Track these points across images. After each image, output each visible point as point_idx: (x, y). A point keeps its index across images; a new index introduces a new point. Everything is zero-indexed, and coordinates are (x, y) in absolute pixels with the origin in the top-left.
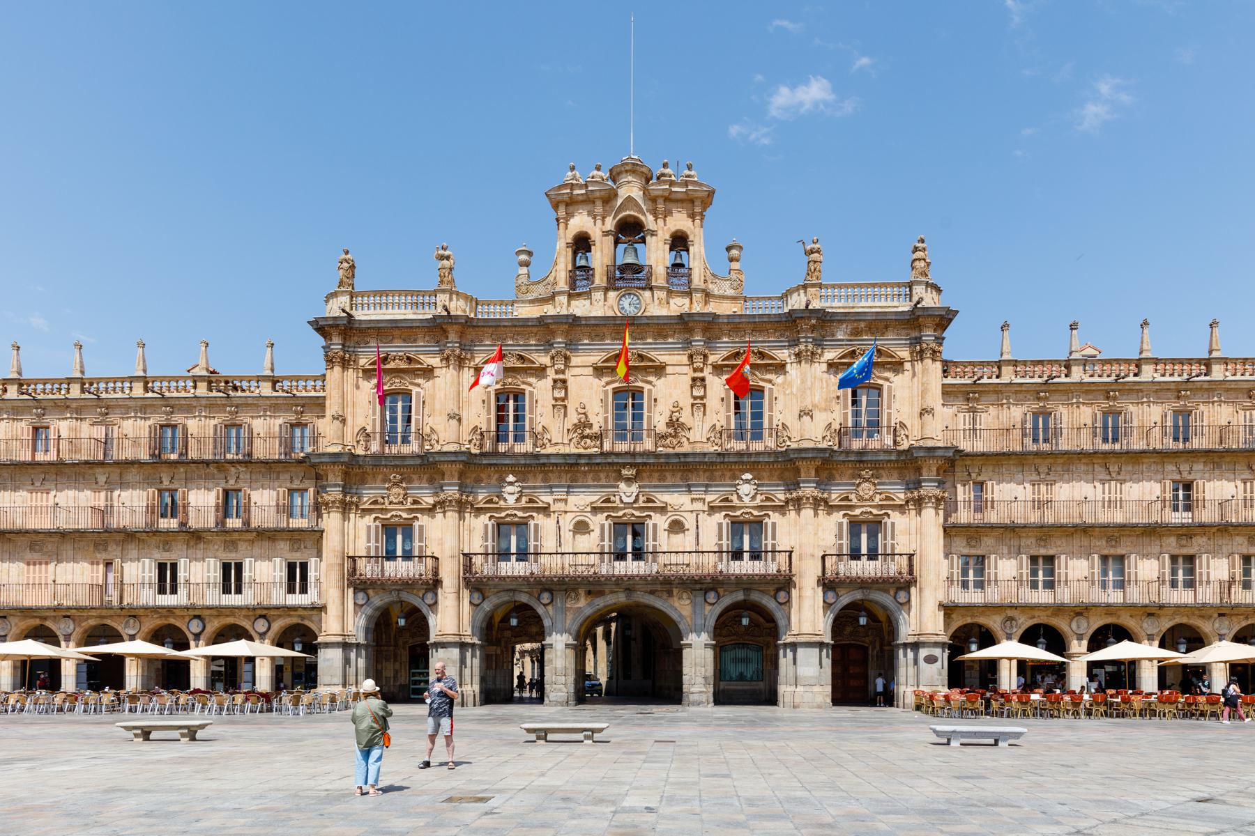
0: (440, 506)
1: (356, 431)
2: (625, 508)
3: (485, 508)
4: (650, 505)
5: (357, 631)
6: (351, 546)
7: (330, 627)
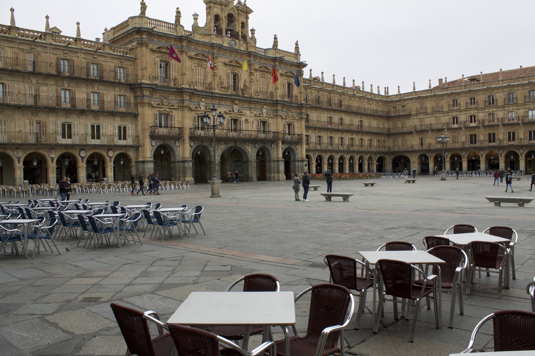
0: (182, 107)
2: (234, 114)
3: (194, 110)
4: (241, 114)
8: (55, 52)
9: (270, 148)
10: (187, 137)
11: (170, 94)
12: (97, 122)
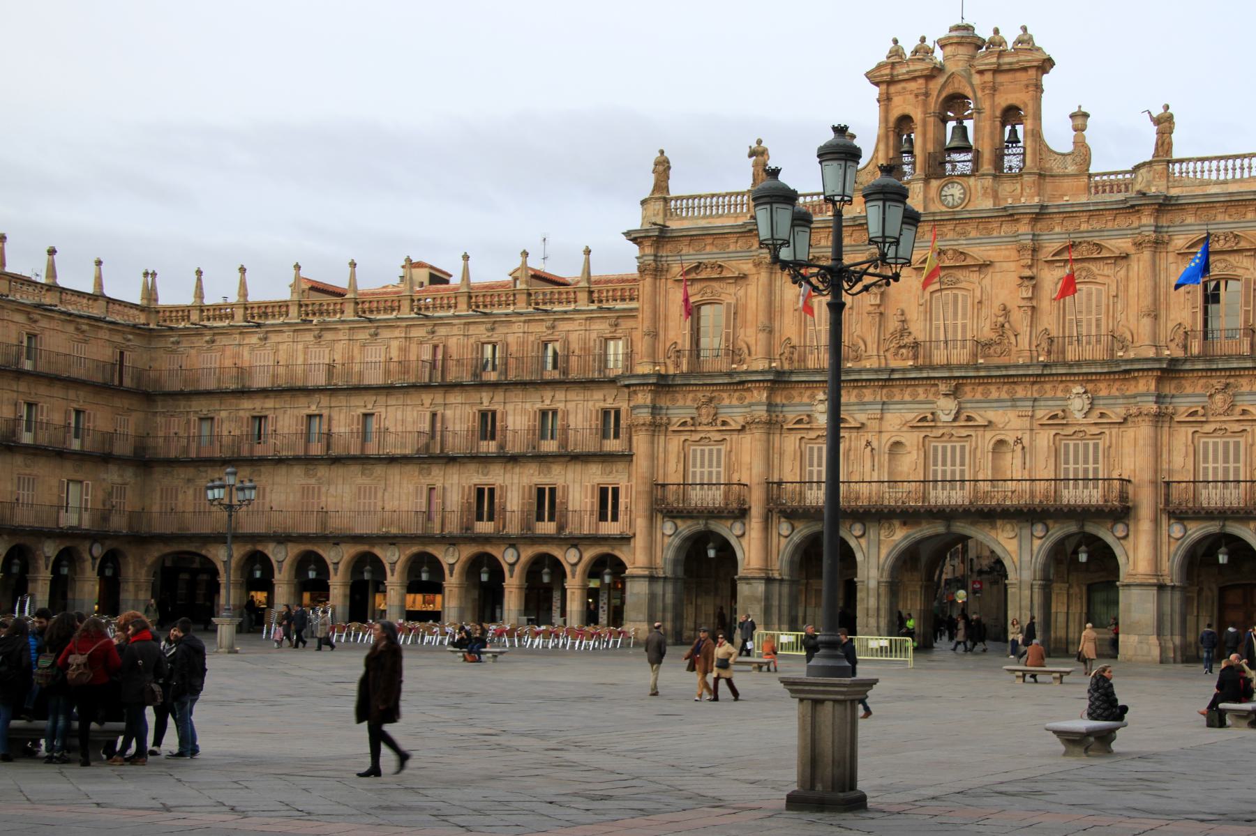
1: (668, 345)
2: (944, 427)
4: (970, 424)
5: (665, 563)
6: (661, 472)
7: (635, 559)
8: (473, 330)
9: (1109, 539)
10: (756, 510)
11: (722, 391)
12: (546, 480)
